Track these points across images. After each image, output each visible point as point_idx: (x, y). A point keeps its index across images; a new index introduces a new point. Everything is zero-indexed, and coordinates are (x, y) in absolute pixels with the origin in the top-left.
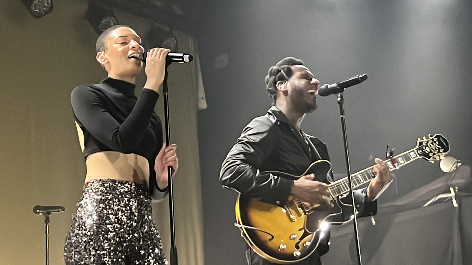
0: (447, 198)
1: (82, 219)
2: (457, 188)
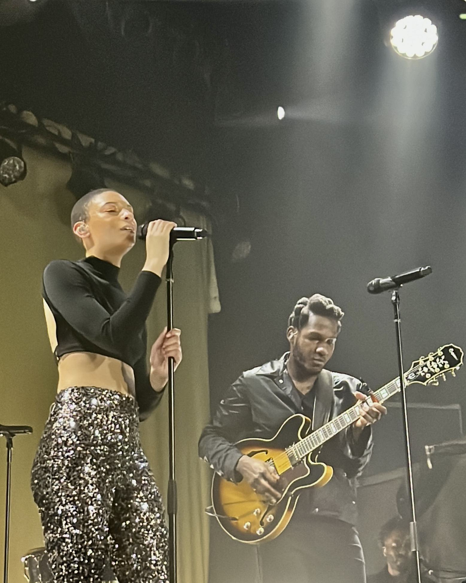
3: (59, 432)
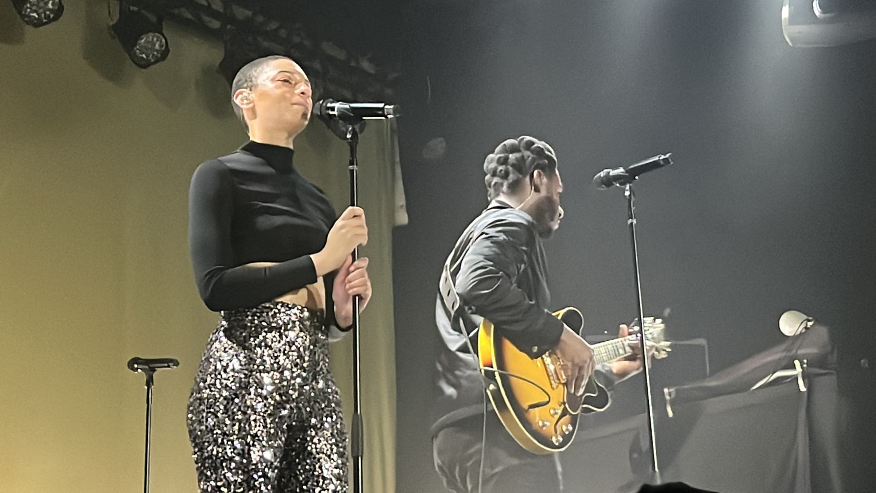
0: (788, 377)
1: (220, 361)
2: (805, 361)
3: (218, 354)
